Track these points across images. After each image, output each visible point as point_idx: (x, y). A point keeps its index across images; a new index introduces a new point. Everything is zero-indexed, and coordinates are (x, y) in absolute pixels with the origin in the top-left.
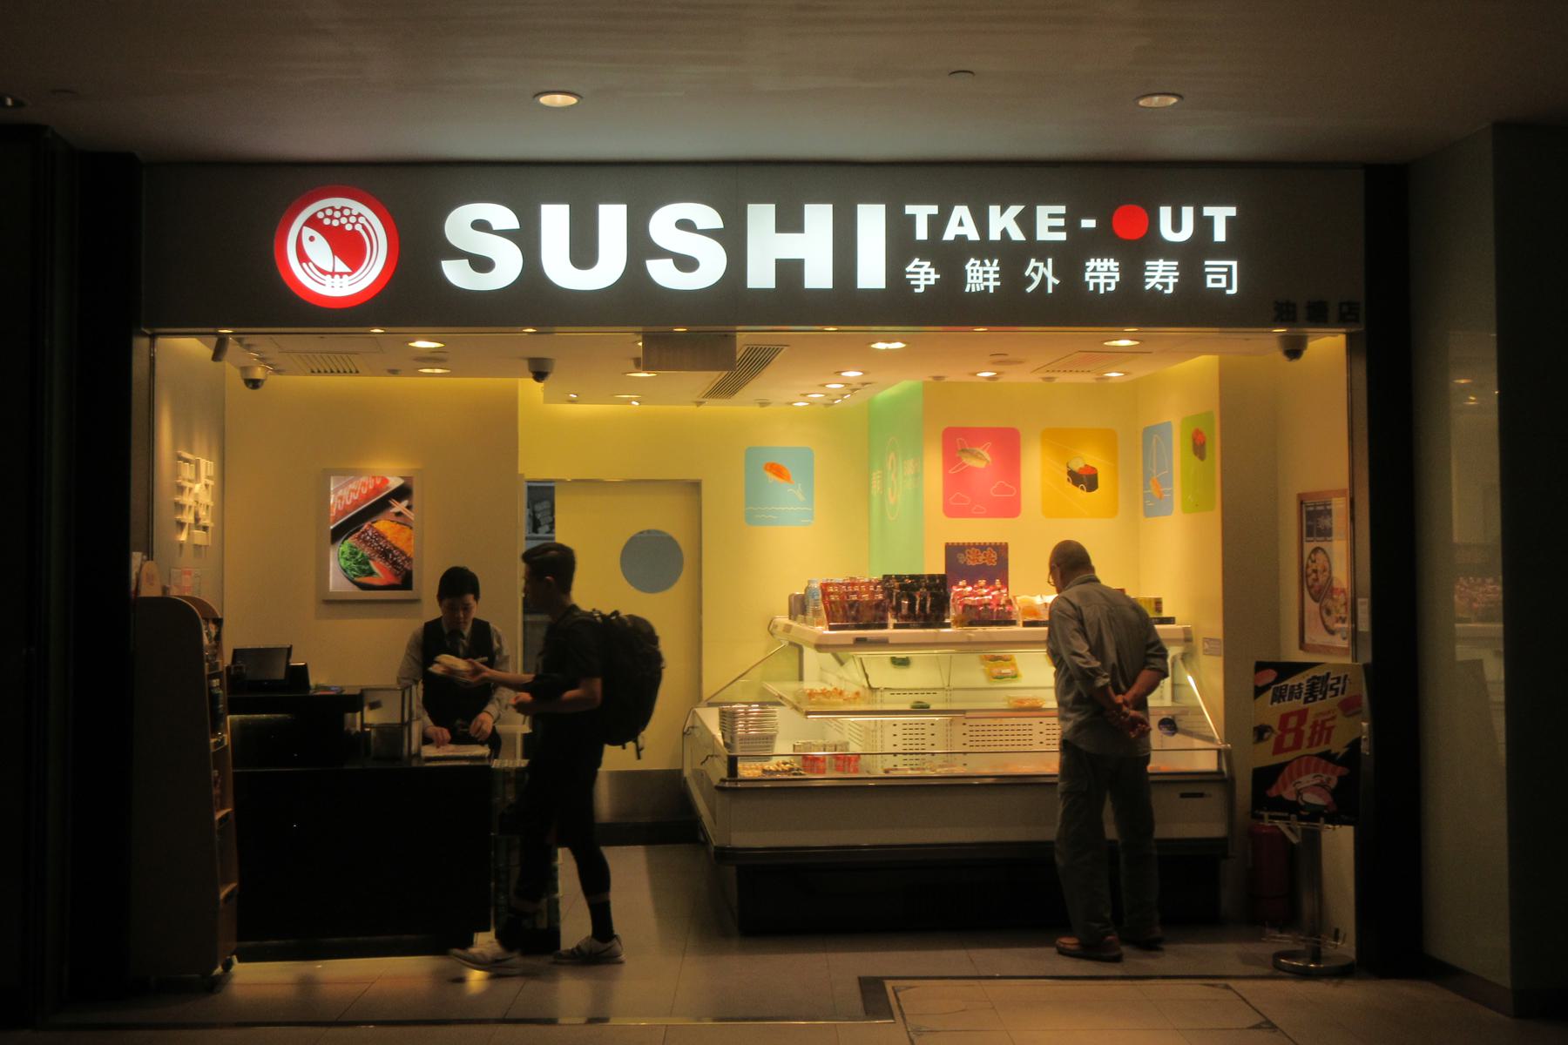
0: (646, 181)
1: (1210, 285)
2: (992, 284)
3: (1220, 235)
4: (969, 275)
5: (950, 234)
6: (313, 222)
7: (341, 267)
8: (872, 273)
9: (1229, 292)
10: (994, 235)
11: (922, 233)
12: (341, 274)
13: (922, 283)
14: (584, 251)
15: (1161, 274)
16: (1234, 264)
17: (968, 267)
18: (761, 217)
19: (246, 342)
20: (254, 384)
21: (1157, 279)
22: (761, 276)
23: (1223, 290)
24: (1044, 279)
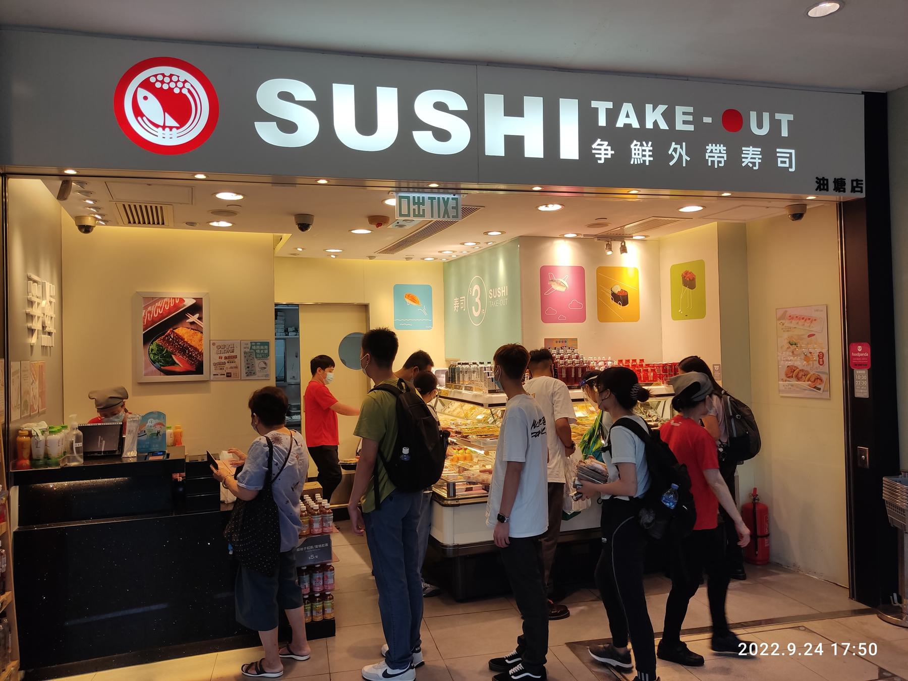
0: (413, 70)
1: (780, 165)
2: (648, 159)
3: (785, 133)
4: (633, 152)
5: (620, 124)
6: (146, 85)
7: (171, 122)
8: (569, 149)
9: (790, 170)
10: (649, 125)
11: (602, 122)
12: (171, 128)
13: (603, 157)
14: (366, 122)
15: (751, 156)
16: (793, 151)
17: (632, 146)
18: (494, 104)
19: (87, 188)
20: (87, 229)
21: (749, 160)
22: (495, 147)
23: (787, 168)
24: (681, 156)
